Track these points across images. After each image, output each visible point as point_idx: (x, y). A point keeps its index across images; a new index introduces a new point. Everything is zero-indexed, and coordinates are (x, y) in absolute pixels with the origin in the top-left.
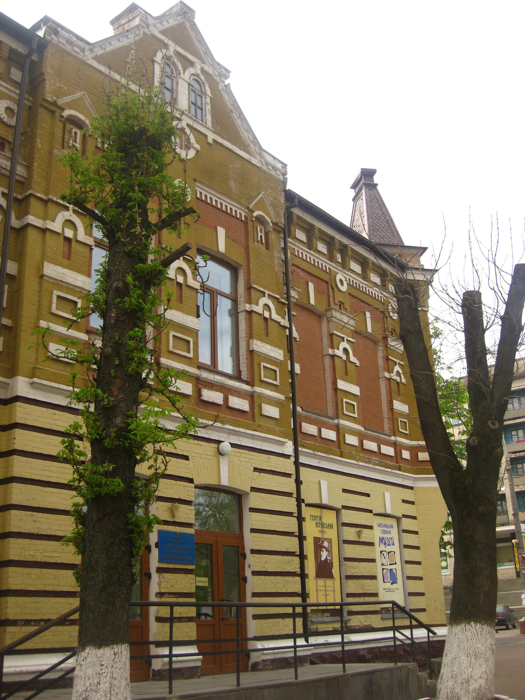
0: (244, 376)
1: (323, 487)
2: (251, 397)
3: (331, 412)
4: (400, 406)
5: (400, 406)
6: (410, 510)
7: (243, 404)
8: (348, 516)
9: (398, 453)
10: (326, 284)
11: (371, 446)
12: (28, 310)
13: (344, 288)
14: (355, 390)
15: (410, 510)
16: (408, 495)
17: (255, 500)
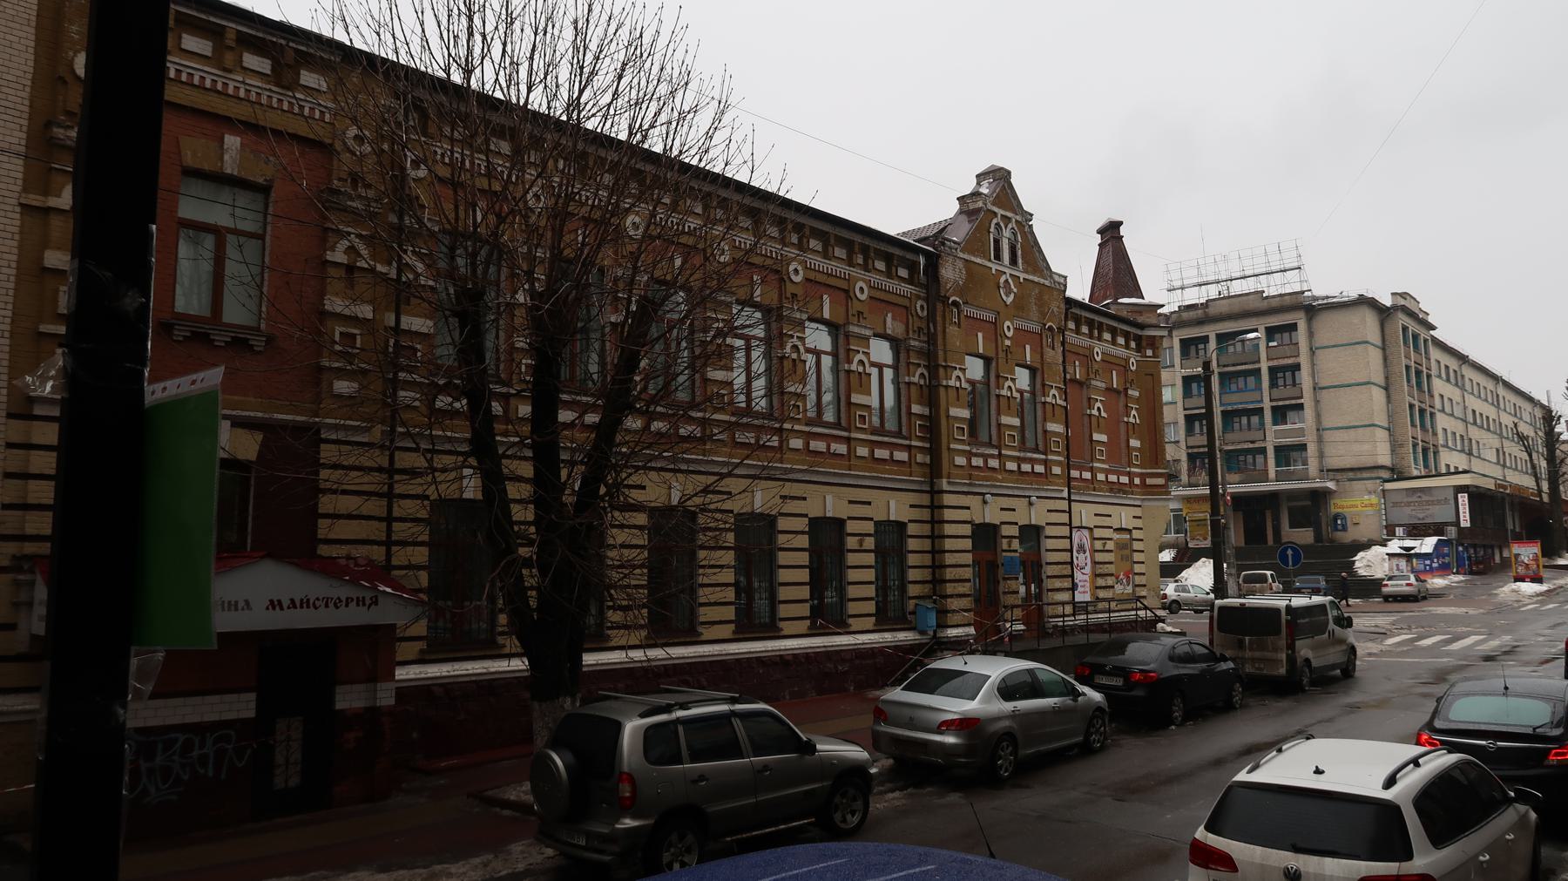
3: (1088, 457)
4: (1135, 443)
5: (1135, 443)
6: (1138, 523)
7: (1040, 469)
8: (1098, 533)
9: (1131, 481)
10: (1087, 357)
13: (1098, 359)
14: (1104, 438)
15: (1138, 523)
16: (1138, 512)
17: (1050, 531)
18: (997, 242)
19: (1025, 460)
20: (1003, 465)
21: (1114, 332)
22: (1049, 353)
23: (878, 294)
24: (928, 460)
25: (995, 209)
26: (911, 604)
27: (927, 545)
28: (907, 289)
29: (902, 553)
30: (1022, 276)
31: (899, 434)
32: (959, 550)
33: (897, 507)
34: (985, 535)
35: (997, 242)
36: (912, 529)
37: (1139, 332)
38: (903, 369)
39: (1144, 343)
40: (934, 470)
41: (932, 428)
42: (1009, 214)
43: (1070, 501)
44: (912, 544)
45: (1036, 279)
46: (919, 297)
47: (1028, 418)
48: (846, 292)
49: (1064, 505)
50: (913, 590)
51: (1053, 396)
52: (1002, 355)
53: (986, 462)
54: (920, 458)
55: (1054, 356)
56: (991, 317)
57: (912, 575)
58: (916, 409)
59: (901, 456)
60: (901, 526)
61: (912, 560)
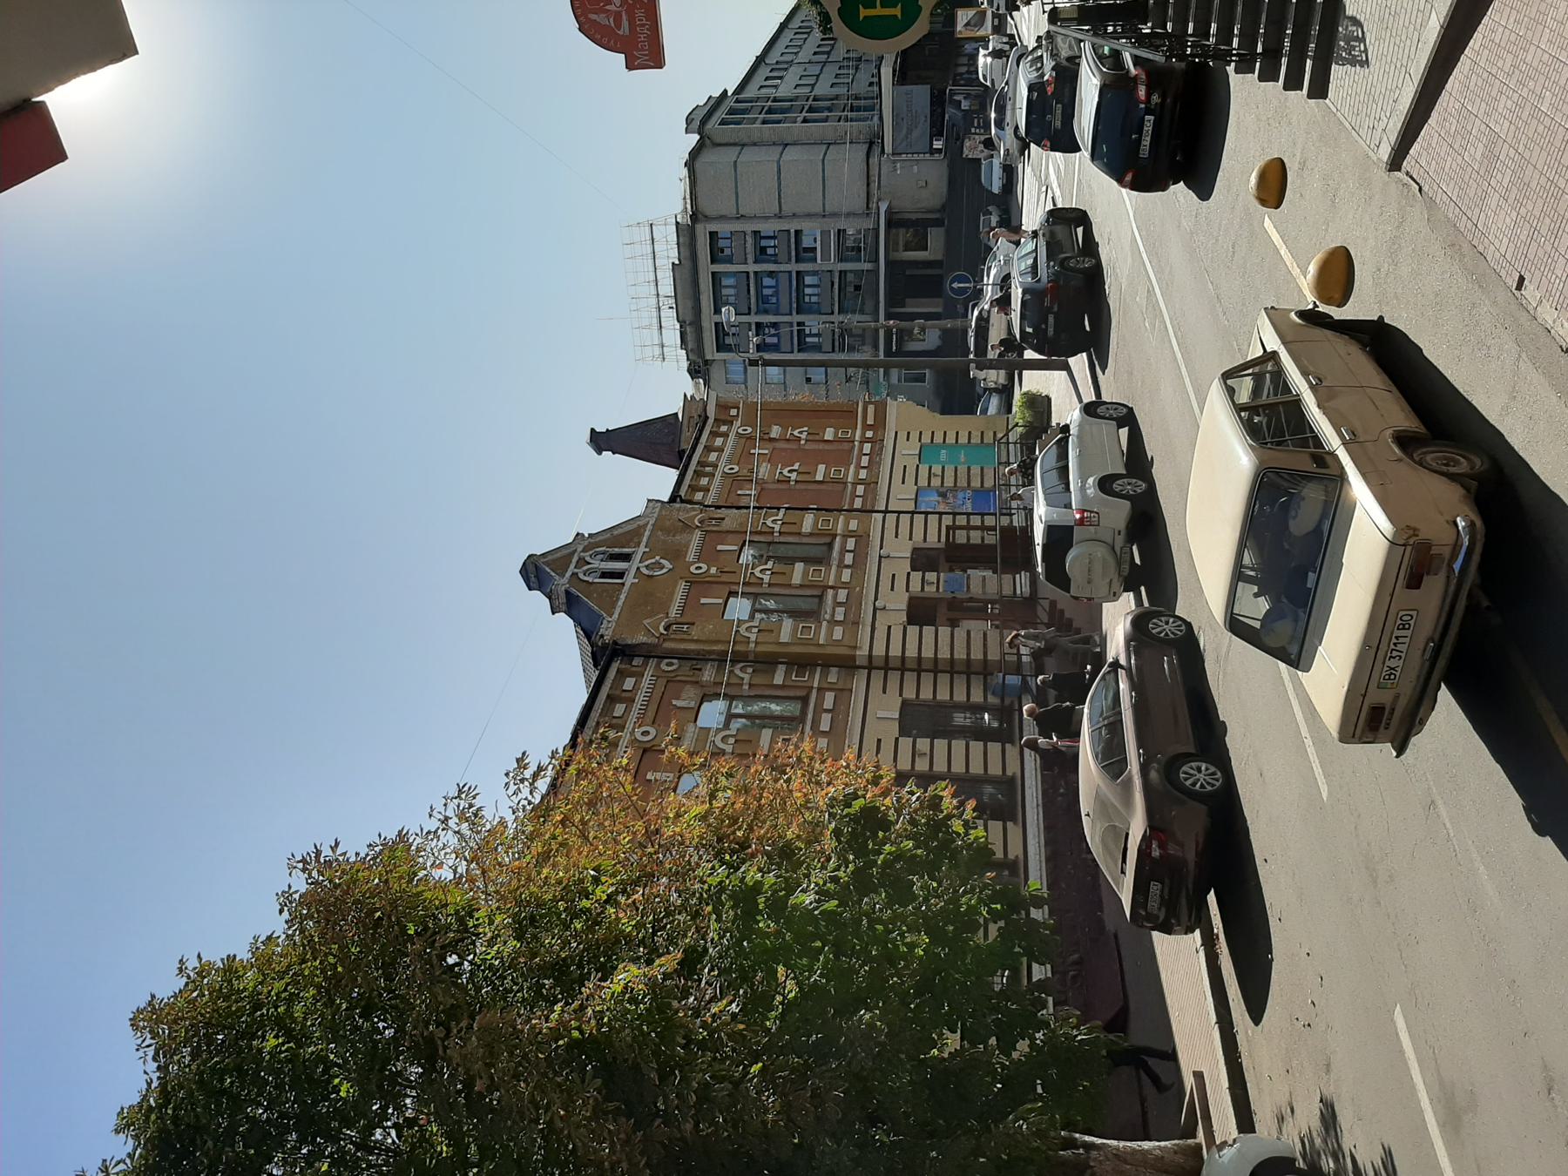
0: (828, 540)
1: (902, 496)
2: (845, 537)
4: (829, 434)
5: (829, 434)
6: (914, 436)
7: (851, 543)
8: (923, 482)
9: (868, 440)
10: (735, 480)
11: (865, 461)
12: (813, 650)
13: (736, 468)
14: (821, 468)
15: (914, 436)
16: (902, 436)
18: (604, 575)
19: (841, 560)
20: (845, 585)
21: (709, 449)
22: (727, 525)
23: (651, 714)
24: (834, 670)
25: (568, 574)
26: (992, 700)
27: (927, 679)
28: (646, 682)
29: (936, 707)
30: (642, 549)
31: (805, 700)
32: (933, 642)
33: (887, 708)
34: (920, 612)
35: (604, 575)
36: (910, 694)
37: (711, 421)
38: (732, 692)
39: (722, 417)
40: (847, 664)
41: (802, 663)
42: (575, 560)
43: (886, 512)
44: (927, 694)
45: (647, 533)
46: (658, 665)
47: (800, 552)
48: (645, 751)
49: (891, 518)
50: (977, 697)
51: (775, 522)
52: (725, 578)
53: (840, 604)
54: (832, 678)
55: (731, 519)
56: (682, 586)
57: (960, 697)
58: (779, 679)
59: (829, 699)
60: (905, 704)
61: (943, 695)
